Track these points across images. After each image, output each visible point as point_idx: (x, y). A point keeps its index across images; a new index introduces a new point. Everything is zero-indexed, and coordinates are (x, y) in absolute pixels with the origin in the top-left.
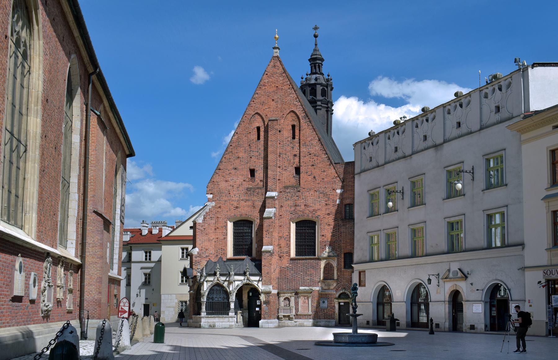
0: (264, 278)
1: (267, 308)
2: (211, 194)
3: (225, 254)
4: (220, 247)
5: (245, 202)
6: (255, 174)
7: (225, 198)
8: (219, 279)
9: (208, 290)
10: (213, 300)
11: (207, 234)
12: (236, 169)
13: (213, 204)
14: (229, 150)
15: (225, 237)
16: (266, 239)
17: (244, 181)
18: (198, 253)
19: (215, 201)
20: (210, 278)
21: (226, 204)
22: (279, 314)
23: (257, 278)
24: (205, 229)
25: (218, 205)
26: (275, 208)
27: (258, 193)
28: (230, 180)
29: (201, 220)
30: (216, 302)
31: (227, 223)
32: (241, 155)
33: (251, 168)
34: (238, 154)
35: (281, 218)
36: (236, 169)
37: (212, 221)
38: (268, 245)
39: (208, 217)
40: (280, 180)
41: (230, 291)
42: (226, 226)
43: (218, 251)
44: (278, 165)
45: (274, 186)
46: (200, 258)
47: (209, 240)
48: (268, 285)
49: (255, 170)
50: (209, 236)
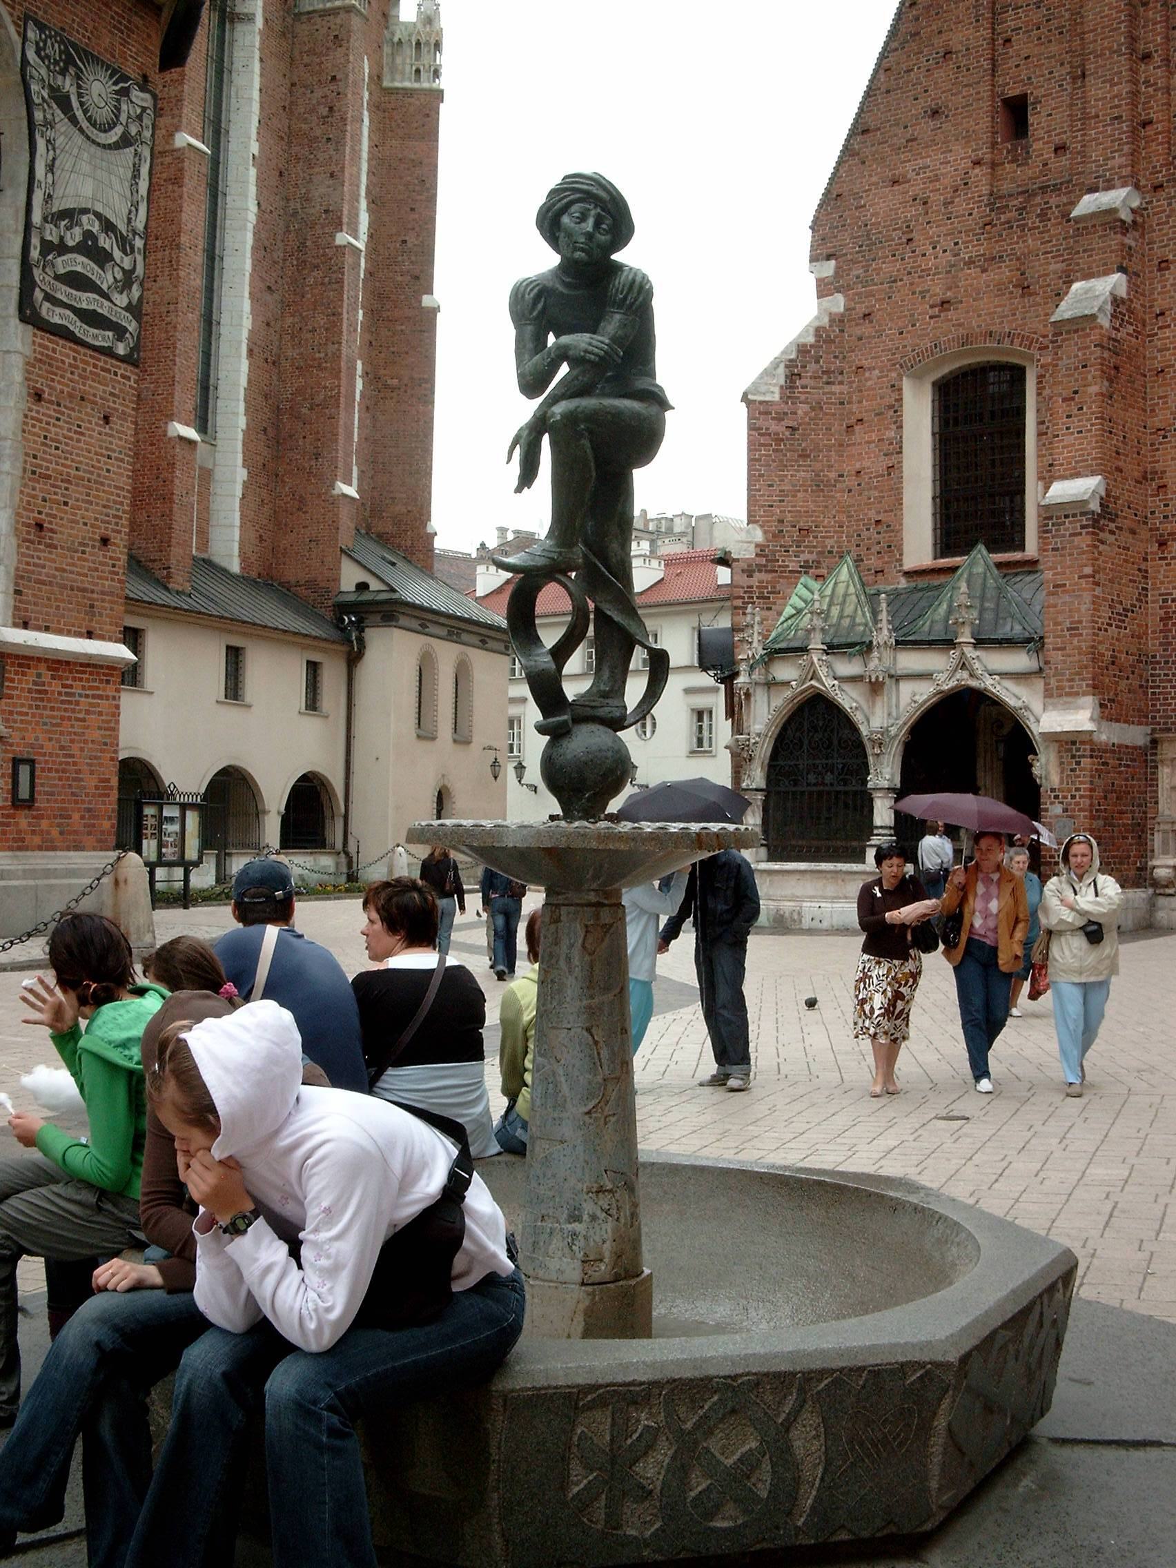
0: (1056, 657)
1: (1069, 822)
2: (829, 257)
3: (893, 548)
4: (873, 515)
5: (984, 271)
6: (1031, 119)
7: (889, 268)
8: (822, 672)
9: (774, 731)
10: (796, 783)
11: (804, 456)
12: (935, 113)
13: (838, 303)
14: (903, 29)
15: (893, 460)
16: (1069, 440)
17: (977, 163)
18: (761, 550)
19: (849, 288)
20: (785, 671)
21: (896, 297)
22: (1155, 862)
23: (1020, 661)
24: (793, 429)
25: (862, 309)
26: (1121, 269)
27: (1043, 216)
28: (911, 175)
29: (777, 390)
30: (811, 793)
31: (900, 390)
32: (957, 39)
33: (1011, 93)
34: (944, 37)
35: (1160, 328)
36: (935, 113)
37: (836, 388)
38: (1077, 475)
39: (811, 367)
40: (1150, 122)
41: (872, 733)
42: (896, 408)
43: (865, 534)
44: (1141, 47)
45: (1118, 160)
46: (769, 577)
47: (819, 485)
48: (1077, 694)
49: (1031, 99)
50: (818, 466)
